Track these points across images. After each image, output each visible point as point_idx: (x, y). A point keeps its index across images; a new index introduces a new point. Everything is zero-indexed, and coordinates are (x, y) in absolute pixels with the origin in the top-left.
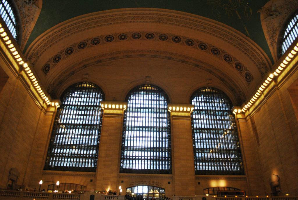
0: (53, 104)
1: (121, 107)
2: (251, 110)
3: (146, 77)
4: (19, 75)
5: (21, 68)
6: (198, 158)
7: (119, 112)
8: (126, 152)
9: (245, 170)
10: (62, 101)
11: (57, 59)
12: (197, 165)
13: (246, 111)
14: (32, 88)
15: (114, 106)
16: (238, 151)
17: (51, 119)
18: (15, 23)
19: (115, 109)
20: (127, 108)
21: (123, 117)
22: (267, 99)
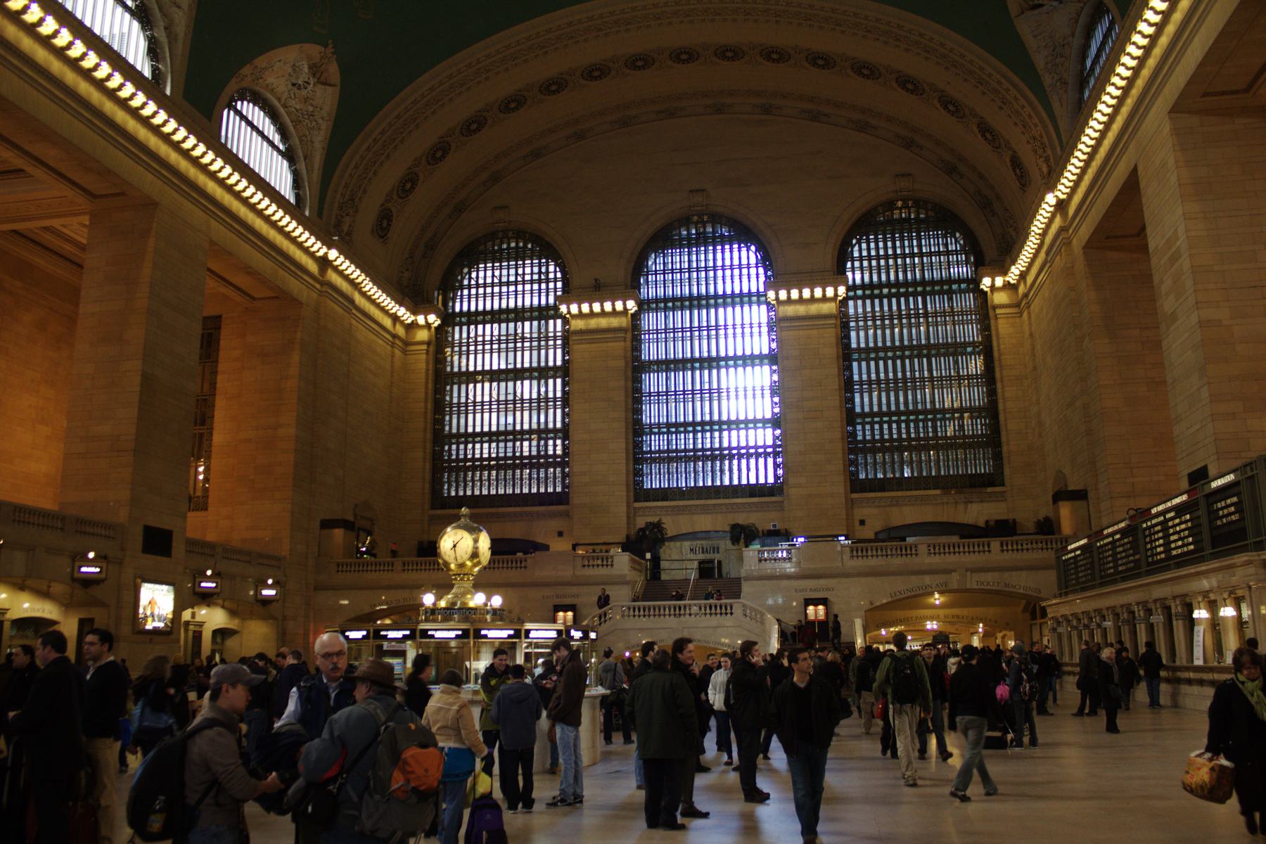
0: (421, 320)
1: (619, 306)
2: (1030, 279)
4: (322, 284)
5: (324, 262)
6: (860, 442)
7: (615, 322)
9: (1007, 471)
10: (445, 304)
11: (408, 185)
12: (854, 463)
13: (1019, 281)
14: (358, 298)
15: (597, 307)
16: (991, 411)
17: (423, 366)
18: (281, 147)
20: (641, 304)
21: (629, 335)
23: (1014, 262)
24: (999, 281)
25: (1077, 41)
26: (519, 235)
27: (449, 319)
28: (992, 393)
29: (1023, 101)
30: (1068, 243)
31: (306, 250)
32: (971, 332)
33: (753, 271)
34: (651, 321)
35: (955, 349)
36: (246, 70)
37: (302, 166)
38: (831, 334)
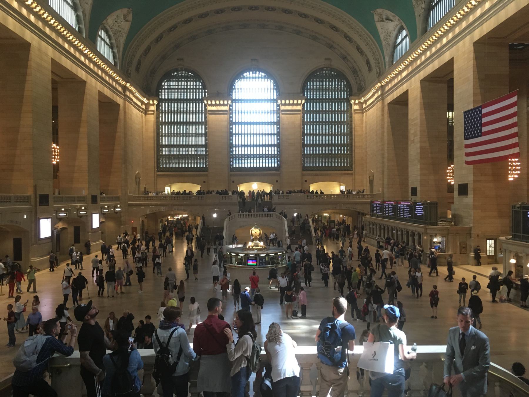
0: (151, 102)
1: (226, 102)
2: (368, 103)
3: (252, 60)
5: (125, 88)
8: (234, 149)
18: (109, 44)
19: (220, 105)
22: (377, 103)
23: (363, 96)
24: (357, 101)
25: (395, 33)
26: (188, 70)
27: (160, 101)
28: (351, 139)
29: (374, 46)
30: (383, 99)
31: (119, 84)
32: (344, 117)
33: (272, 91)
34: (237, 107)
35: (340, 123)
36: (104, 22)
37: (115, 50)
38: (299, 117)
